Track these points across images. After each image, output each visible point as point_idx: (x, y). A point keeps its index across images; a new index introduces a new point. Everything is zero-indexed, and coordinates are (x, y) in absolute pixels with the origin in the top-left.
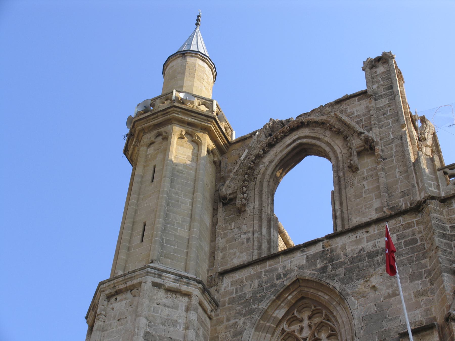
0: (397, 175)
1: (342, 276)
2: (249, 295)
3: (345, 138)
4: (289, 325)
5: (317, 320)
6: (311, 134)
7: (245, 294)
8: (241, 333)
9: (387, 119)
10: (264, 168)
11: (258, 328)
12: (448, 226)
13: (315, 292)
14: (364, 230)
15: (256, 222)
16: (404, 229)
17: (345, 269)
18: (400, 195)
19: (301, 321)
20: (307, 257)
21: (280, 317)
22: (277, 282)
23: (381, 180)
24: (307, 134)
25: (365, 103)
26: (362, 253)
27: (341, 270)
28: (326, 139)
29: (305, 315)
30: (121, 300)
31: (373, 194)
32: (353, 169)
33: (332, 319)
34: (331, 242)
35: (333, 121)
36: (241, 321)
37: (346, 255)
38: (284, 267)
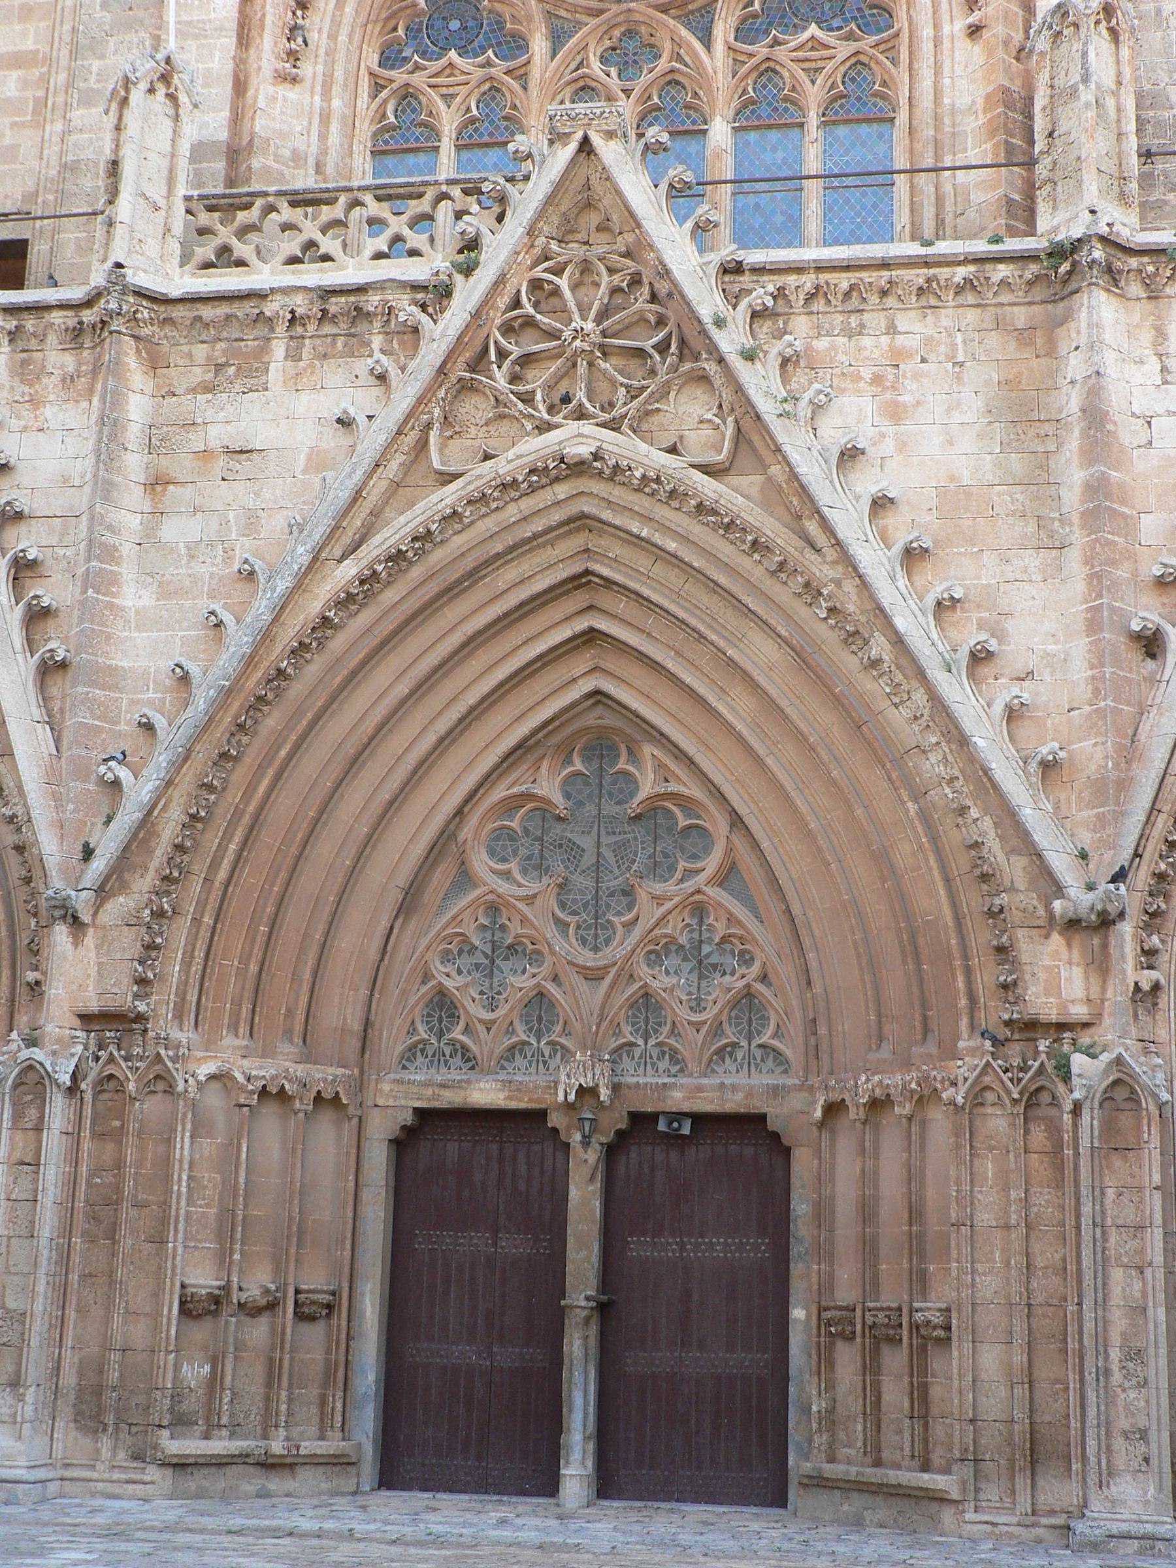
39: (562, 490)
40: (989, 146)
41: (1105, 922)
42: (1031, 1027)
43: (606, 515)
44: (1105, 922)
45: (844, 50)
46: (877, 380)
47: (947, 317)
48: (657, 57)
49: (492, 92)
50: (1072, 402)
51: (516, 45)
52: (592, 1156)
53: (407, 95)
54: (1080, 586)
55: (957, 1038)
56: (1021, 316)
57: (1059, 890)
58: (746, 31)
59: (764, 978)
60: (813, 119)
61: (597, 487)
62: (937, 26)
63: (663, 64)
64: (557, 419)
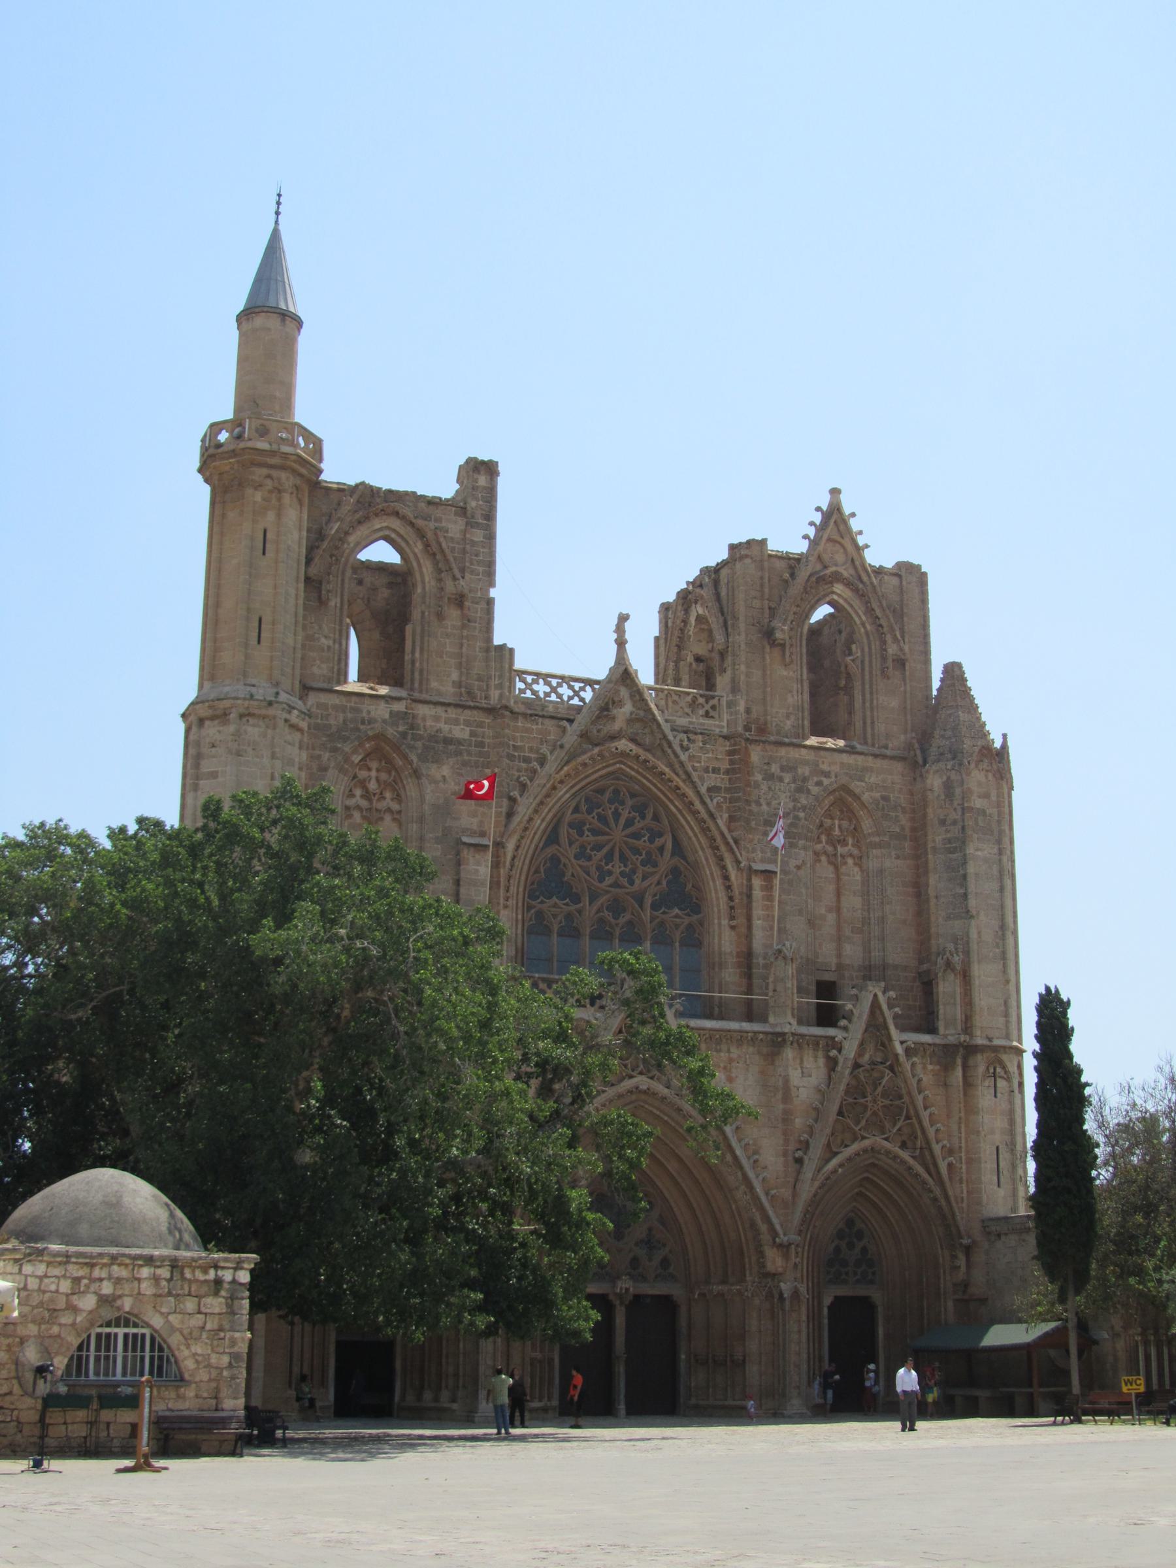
0: (477, 649)
1: (420, 751)
2: (334, 729)
3: (440, 571)
4: (360, 769)
5: (384, 776)
6: (402, 532)
7: (330, 725)
8: (325, 769)
9: (478, 565)
10: (347, 551)
11: (341, 770)
12: (511, 743)
13: (391, 752)
14: (444, 708)
15: (337, 627)
16: (477, 726)
17: (423, 744)
18: (475, 677)
19: (369, 769)
20: (391, 712)
21: (357, 761)
22: (362, 727)
23: (464, 650)
24: (398, 529)
25: (461, 522)
26: (439, 734)
27: (419, 744)
28: (416, 550)
29: (374, 765)
30: (254, 726)
31: (453, 661)
32: (440, 616)
33: (400, 785)
34: (414, 705)
35: (430, 535)
36: (326, 756)
37: (424, 727)
38: (369, 712)
39: (634, 1097)
40: (738, 970)
41: (790, 1244)
42: (767, 1275)
43: (646, 1106)
44: (790, 1244)
45: (687, 921)
46: (725, 1068)
47: (745, 1047)
48: (624, 910)
49: (569, 917)
50: (780, 1083)
51: (576, 899)
52: (623, 1308)
53: (540, 915)
54: (781, 1142)
55: (745, 1276)
56: (765, 1050)
57: (774, 1234)
58: (654, 907)
59: (670, 1251)
60: (677, 944)
61: (643, 1097)
62: (719, 918)
63: (627, 917)
64: (634, 1074)
